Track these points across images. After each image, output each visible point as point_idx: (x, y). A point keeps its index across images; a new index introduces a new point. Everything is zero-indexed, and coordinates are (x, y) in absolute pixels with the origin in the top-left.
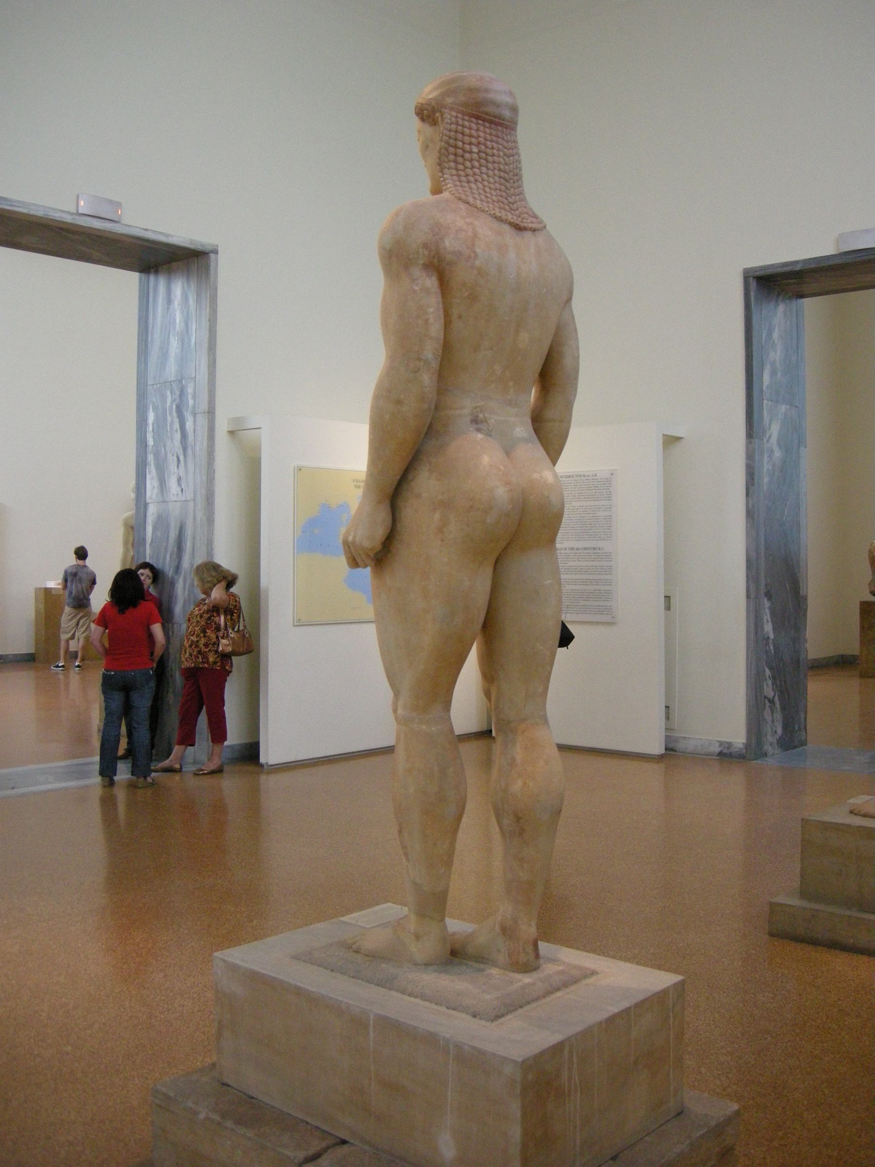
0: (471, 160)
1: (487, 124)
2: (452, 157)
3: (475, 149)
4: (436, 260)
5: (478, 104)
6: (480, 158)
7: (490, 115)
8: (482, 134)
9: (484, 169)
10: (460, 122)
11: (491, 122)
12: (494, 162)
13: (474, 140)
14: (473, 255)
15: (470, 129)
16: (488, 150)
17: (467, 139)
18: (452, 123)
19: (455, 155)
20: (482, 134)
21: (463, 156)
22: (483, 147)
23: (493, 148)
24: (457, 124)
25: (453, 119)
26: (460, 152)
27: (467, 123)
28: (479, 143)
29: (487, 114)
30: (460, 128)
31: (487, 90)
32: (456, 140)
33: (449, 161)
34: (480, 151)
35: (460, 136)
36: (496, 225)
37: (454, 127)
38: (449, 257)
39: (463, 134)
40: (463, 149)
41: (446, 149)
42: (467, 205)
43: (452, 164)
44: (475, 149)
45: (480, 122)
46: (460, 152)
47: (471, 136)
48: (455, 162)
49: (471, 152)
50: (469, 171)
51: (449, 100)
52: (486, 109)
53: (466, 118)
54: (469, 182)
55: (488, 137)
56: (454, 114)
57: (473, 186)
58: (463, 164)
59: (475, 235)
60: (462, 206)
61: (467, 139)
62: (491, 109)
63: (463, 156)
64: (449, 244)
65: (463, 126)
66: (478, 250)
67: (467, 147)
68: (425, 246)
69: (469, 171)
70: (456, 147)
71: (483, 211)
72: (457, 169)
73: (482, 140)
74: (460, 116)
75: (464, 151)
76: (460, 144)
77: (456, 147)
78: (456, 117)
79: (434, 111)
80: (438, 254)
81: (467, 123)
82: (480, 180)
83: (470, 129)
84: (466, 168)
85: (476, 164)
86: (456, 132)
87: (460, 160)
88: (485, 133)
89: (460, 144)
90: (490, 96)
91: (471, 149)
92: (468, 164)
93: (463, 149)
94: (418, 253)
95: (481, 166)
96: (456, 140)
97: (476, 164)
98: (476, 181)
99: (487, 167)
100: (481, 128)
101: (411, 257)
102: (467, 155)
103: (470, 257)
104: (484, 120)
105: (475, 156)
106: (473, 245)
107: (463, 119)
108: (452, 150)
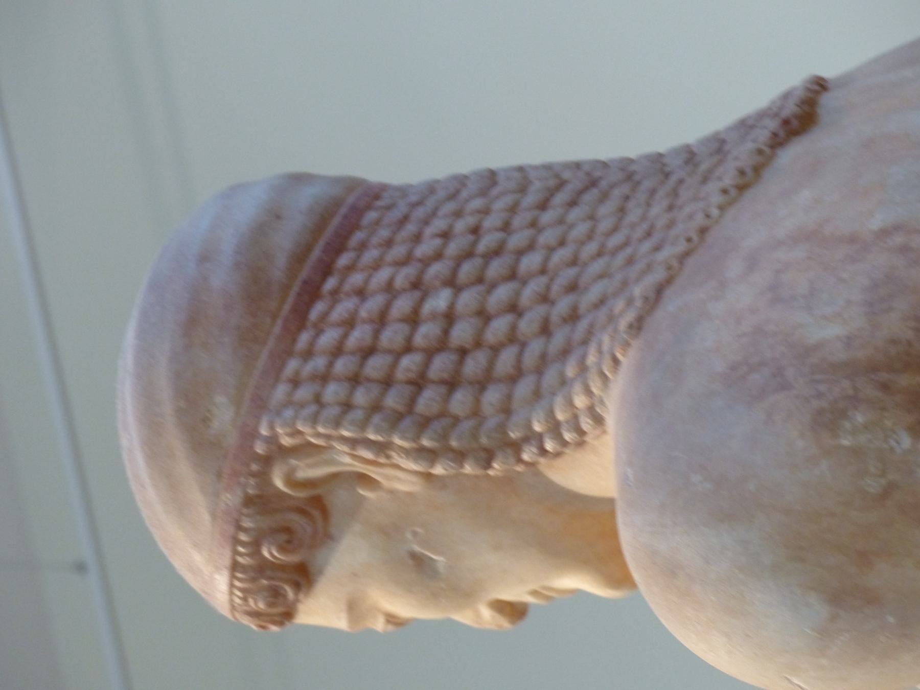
0: (484, 316)
1: (343, 260)
2: (460, 401)
3: (440, 301)
4: (904, 381)
5: (255, 287)
6: (480, 280)
7: (309, 248)
8: (383, 275)
9: (531, 262)
10: (319, 363)
11: (337, 246)
12: (506, 227)
13: (402, 305)
14: (898, 239)
15: (350, 323)
16: (452, 249)
17: (392, 335)
18: (318, 400)
19: (451, 384)
20: (383, 275)
21: (463, 352)
22: (437, 269)
23: (446, 235)
24: (324, 378)
25: (304, 393)
26: (441, 365)
27: (329, 338)
28: (416, 284)
29: (299, 257)
30: (342, 366)
31: (205, 258)
32: (387, 382)
33: (476, 412)
34: (451, 282)
35: (376, 366)
36: (771, 184)
37: (332, 392)
38: (895, 324)
39: (368, 352)
40: (430, 353)
41: (424, 423)
42: (669, 292)
43: (492, 396)
44: (440, 301)
45: (330, 284)
46: (441, 365)
47: (381, 320)
48: (481, 385)
49: (449, 318)
50: (528, 325)
51: (224, 416)
52: (281, 260)
53: (304, 338)
54: (573, 317)
55: (399, 251)
56: (280, 392)
57: (594, 294)
58: (496, 350)
59: (808, 236)
60: (671, 304)
61: (392, 335)
62: (283, 242)
63: (463, 352)
64: (833, 321)
65: (337, 351)
66: (876, 223)
67: (427, 332)
68: (828, 420)
69: (528, 325)
70: (418, 383)
71: (703, 231)
72: (514, 379)
73: (402, 278)
74: (292, 365)
75: (441, 345)
76: (409, 363)
77: (418, 383)
78: (295, 383)
79: (262, 502)
80: (872, 368)
81: (329, 338)
82: (572, 272)
83: (350, 323)
84: (512, 337)
85: (503, 293)
86: (355, 380)
87: (473, 366)
88: (376, 266)
89: (409, 363)
90: (228, 245)
91: (434, 316)
92: (499, 327)
93: (430, 353)
94: (856, 452)
95: (512, 275)
96: (387, 382)
97: (503, 293)
98: (573, 287)
99: (520, 253)
100: (356, 279)
101: (873, 485)
102: (462, 333)
103: (904, 249)
104: (326, 269)
105: (468, 299)
106: (852, 239)
107: (309, 354)
108: (428, 400)
